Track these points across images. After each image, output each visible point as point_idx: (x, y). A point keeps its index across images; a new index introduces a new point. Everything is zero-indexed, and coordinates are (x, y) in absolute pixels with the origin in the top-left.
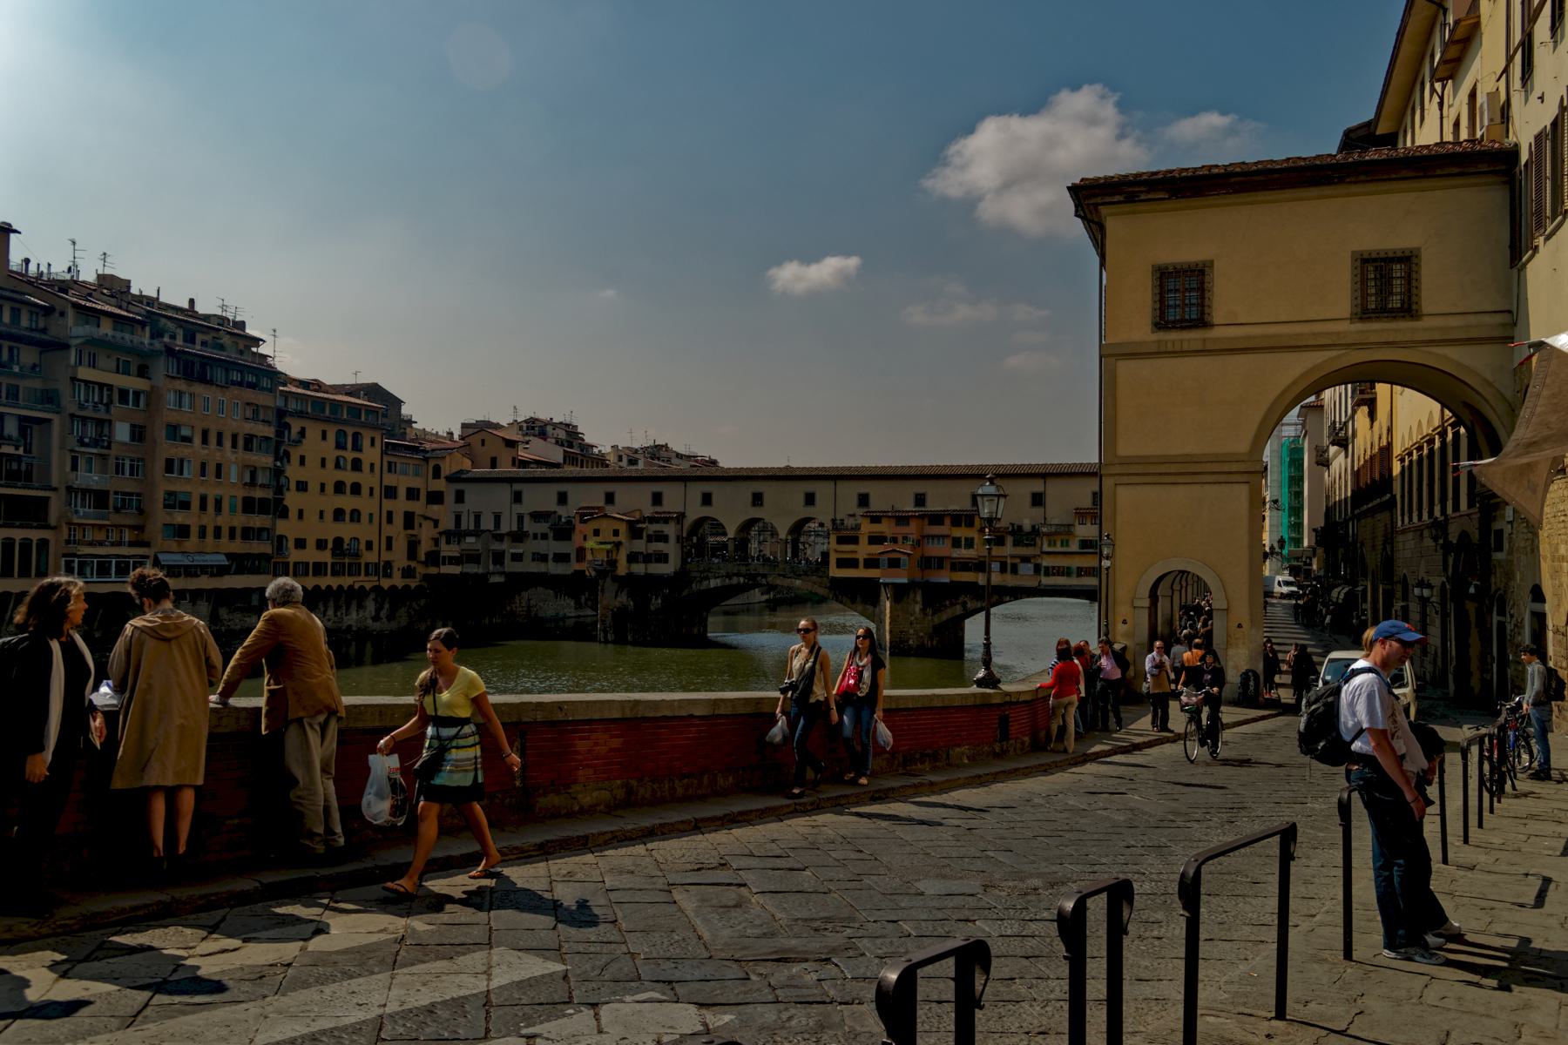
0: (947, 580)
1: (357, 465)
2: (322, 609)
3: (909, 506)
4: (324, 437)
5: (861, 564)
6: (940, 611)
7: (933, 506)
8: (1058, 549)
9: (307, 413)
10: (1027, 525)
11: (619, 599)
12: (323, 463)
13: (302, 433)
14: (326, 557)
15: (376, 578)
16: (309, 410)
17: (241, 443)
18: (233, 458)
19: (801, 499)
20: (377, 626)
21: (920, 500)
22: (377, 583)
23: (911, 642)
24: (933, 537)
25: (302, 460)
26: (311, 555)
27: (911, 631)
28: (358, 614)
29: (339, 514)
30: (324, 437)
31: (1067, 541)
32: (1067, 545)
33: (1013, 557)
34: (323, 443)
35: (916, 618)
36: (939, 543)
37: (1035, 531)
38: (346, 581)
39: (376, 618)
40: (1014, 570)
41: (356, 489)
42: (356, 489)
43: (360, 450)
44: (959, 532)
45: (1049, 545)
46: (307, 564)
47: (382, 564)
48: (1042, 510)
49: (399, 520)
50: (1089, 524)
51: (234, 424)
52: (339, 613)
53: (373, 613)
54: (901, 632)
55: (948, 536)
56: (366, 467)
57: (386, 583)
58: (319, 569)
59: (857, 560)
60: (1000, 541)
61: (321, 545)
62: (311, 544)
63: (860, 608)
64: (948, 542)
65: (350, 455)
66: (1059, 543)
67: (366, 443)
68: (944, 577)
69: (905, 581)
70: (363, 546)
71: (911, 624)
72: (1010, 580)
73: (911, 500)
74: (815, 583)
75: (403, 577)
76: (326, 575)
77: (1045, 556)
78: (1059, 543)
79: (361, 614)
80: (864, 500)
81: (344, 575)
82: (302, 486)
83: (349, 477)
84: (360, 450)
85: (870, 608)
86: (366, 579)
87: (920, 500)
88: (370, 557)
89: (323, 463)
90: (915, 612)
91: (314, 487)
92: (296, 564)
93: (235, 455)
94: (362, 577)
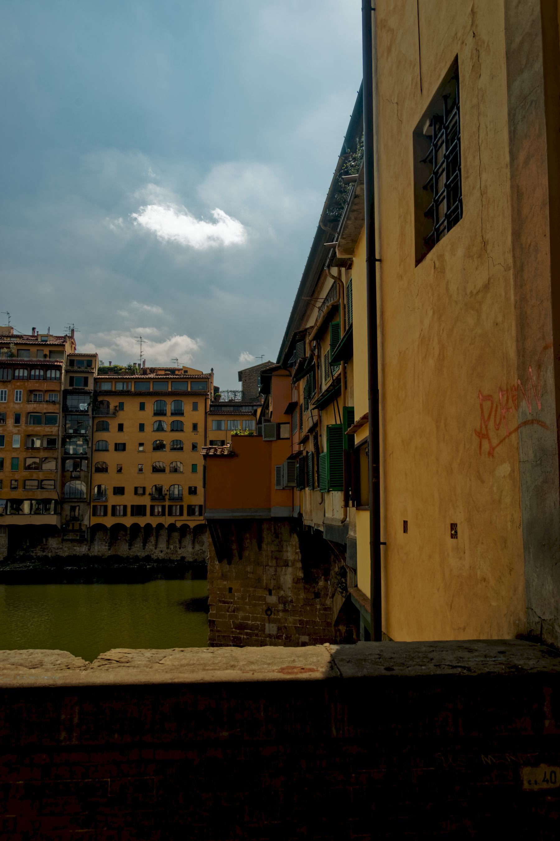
1: (177, 427)
4: (142, 407)
9: (131, 392)
12: (142, 427)
13: (121, 406)
14: (146, 501)
16: (133, 390)
17: (23, 419)
18: (15, 430)
25: (121, 427)
26: (129, 499)
28: (193, 548)
30: (142, 407)
38: (167, 521)
41: (177, 447)
43: (182, 414)
46: (125, 507)
51: (17, 406)
52: (172, 547)
56: (188, 427)
58: (139, 510)
62: (129, 490)
65: (168, 420)
67: (187, 407)
70: (186, 492)
71: (269, 610)
76: (145, 515)
79: (197, 547)
81: (163, 514)
82: (120, 447)
83: (168, 437)
84: (182, 414)
86: (189, 518)
89: (142, 427)
90: (279, 587)
92: (114, 507)
93: (17, 428)
94: (185, 516)
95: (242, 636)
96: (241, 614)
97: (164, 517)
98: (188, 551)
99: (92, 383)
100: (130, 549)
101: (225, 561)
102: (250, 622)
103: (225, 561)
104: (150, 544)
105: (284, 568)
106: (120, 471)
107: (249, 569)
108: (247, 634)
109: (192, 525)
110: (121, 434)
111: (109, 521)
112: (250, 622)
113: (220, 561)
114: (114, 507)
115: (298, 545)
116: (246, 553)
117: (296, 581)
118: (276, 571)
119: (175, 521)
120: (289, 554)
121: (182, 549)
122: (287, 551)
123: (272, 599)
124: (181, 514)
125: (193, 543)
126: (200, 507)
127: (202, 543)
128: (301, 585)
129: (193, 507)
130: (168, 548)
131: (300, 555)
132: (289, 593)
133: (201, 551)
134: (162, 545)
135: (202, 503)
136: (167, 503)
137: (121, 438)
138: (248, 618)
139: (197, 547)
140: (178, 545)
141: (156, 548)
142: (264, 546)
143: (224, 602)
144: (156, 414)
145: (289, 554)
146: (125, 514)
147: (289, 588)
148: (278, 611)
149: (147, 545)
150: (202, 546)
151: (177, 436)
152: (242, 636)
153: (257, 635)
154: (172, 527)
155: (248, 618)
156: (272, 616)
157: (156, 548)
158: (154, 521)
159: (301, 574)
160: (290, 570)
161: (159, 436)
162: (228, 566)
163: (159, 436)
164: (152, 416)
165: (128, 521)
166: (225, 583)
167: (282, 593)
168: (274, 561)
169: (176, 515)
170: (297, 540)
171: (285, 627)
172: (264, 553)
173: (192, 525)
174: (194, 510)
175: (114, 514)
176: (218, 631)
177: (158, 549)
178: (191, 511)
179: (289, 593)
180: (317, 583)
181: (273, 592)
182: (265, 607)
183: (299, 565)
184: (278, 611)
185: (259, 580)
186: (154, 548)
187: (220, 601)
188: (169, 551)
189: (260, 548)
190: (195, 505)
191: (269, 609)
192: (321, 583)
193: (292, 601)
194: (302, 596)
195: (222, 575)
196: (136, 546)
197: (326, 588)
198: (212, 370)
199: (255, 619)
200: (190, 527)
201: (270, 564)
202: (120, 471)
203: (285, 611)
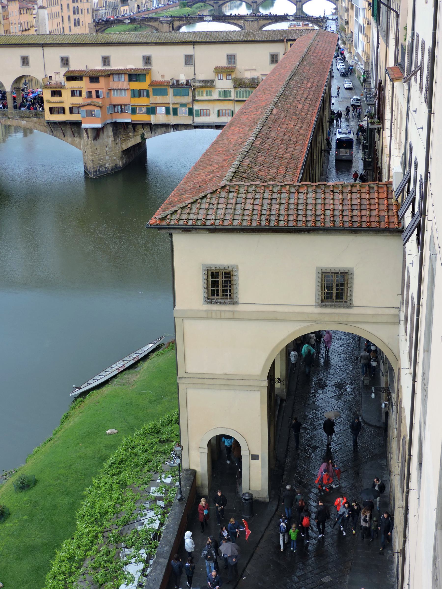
0: (129, 121)
3: (98, 66)
5: (67, 111)
6: (125, 140)
7: (115, 66)
8: (205, 97)
10: (183, 79)
19: (19, 61)
21: (106, 61)
23: (107, 165)
24: (118, 89)
27: (107, 158)
31: (211, 92)
32: (211, 95)
33: (174, 103)
35: (110, 148)
36: (121, 94)
37: (188, 84)
40: (175, 112)
44: (136, 86)
45: (198, 95)
48: (193, 68)
50: (225, 79)
54: (100, 160)
55: (127, 89)
59: (63, 109)
60: (164, 93)
63: (70, 139)
64: (128, 94)
66: (205, 94)
68: (127, 119)
69: (99, 126)
72: (172, 120)
73: (100, 61)
74: (35, 123)
78: (205, 94)
80: (65, 61)
85: (77, 140)
87: (106, 61)
90: (108, 145)
101: (95, 140)
103: (95, 140)
123: (107, 149)
132: (111, 146)
138: (101, 157)
142: (104, 133)
155: (101, 157)
159: (113, 139)
160: (111, 138)
172: (104, 135)
179: (111, 146)
182: (105, 152)
183: (113, 136)
185: (104, 144)
192: (118, 140)
197: (119, 142)
199: (103, 156)
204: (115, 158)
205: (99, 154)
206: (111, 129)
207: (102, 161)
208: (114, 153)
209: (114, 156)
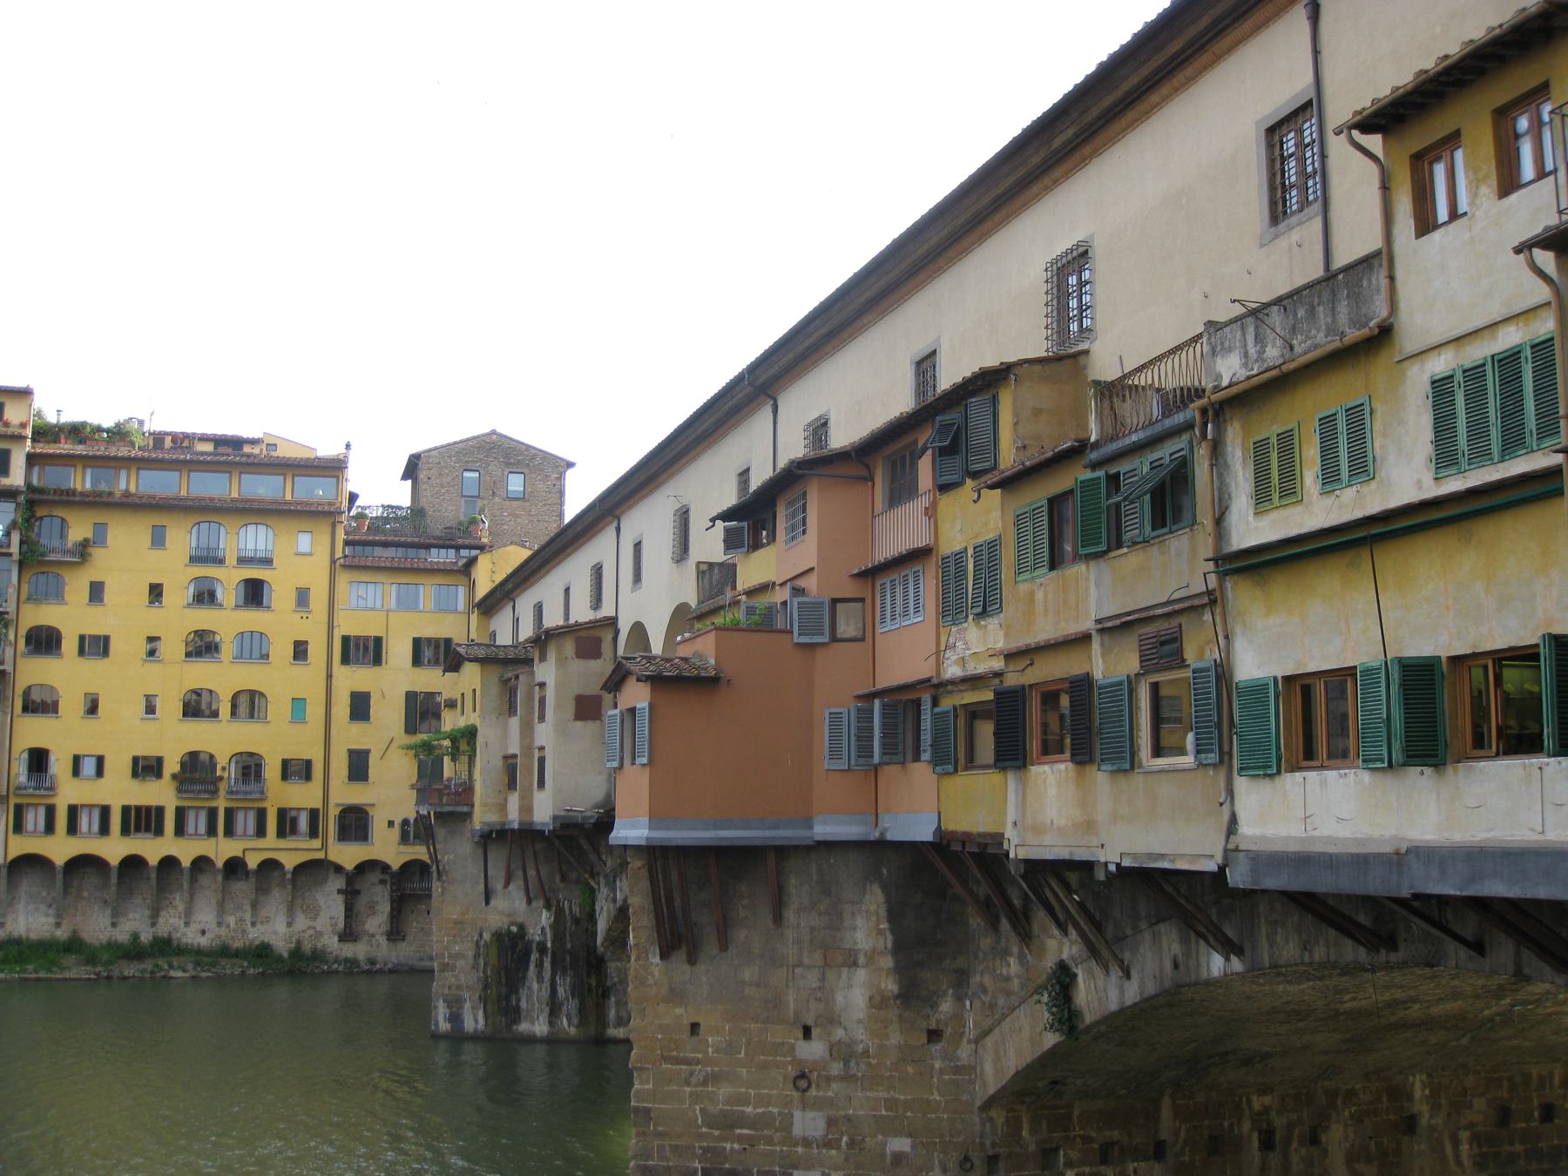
2: (181, 908)
4: (158, 540)
11: (498, 902)
12: (156, 592)
13: (99, 537)
14: (161, 794)
15: (317, 843)
20: (358, 951)
22: (321, 855)
25: (96, 592)
26: (120, 790)
27: (808, 1123)
28: (289, 924)
29: (196, 707)
30: (158, 540)
34: (157, 554)
38: (222, 849)
39: (348, 935)
41: (254, 648)
42: (254, 648)
46: (105, 811)
47: (334, 812)
49: (389, 715)
52: (231, 920)
53: (341, 925)
54: (727, 1122)
55: (918, 555)
57: (348, 855)
58: (143, 820)
61: (146, 768)
75: (405, 838)
76: (159, 831)
77: (1241, 594)
79: (301, 922)
81: (211, 831)
82: (95, 646)
86: (283, 843)
88: (302, 796)
89: (156, 592)
90: (831, 1020)
91: (127, 646)
92: (73, 811)
95: (728, 1146)
96: (723, 1091)
97: (213, 840)
98: (275, 933)
99: (21, 468)
100: (114, 925)
102: (749, 1109)
104: (171, 911)
105: (845, 970)
106: (93, 708)
107: (747, 974)
108: (740, 1139)
109: (290, 861)
110: (96, 610)
111: (60, 849)
112: (749, 1109)
113: (664, 956)
114: (73, 811)
115: (883, 912)
116: (740, 935)
117: (878, 1002)
118: (823, 978)
119: (244, 851)
120: (860, 936)
121: (259, 926)
122: (854, 928)
123: (814, 1050)
124: (261, 831)
125: (291, 910)
126: (314, 814)
127: (313, 912)
128: (892, 1013)
129: (293, 814)
130: (219, 924)
131: (890, 938)
132: (860, 1034)
133: (311, 932)
134: (205, 916)
135: (317, 803)
136: (221, 804)
137: (94, 621)
139: (301, 922)
140: (248, 916)
141: (187, 924)
142: (790, 915)
143: (677, 1061)
144: (195, 560)
145: (860, 936)
146: (104, 829)
147: (859, 1021)
148: (829, 1079)
149: (163, 913)
150: (315, 918)
151: (252, 619)
152: (728, 1146)
153: (770, 1141)
154: (235, 867)
156: (813, 1092)
157: (187, 924)
158: (186, 851)
159: (891, 986)
160: (861, 975)
161: (204, 618)
162: (686, 967)
163: (204, 618)
164: (186, 565)
165: (114, 849)
166: (679, 1011)
167: (840, 1033)
168: (818, 955)
169: (196, 834)
170: (881, 898)
171: (848, 1119)
172: (790, 935)
173: (290, 861)
174: (294, 821)
175: (72, 828)
176: (660, 1135)
177: (194, 927)
178: (287, 823)
179: (860, 1034)
180: (934, 1006)
181: (815, 1032)
182: (791, 1071)
183: (887, 962)
184: (829, 1079)
186: (182, 922)
187: (665, 1059)
188: (223, 931)
189: (778, 918)
190: (299, 809)
191: (803, 1076)
192: (946, 1006)
193: (866, 1053)
194: (895, 1038)
195: (672, 991)
196: (131, 916)
197: (958, 1018)
198: (348, 446)
200: (284, 867)
201: (806, 961)
202: (93, 708)
203: (847, 1078)
204: (901, 1144)
205: (714, 1078)
206: (875, 899)
207: (751, 1142)
208: (891, 1104)
209: (891, 1126)
